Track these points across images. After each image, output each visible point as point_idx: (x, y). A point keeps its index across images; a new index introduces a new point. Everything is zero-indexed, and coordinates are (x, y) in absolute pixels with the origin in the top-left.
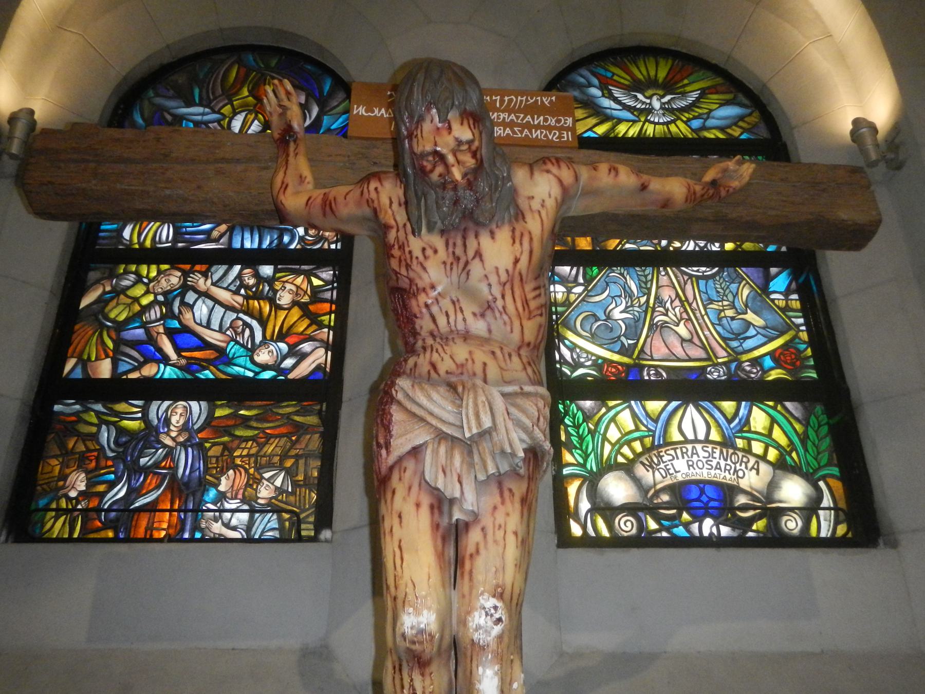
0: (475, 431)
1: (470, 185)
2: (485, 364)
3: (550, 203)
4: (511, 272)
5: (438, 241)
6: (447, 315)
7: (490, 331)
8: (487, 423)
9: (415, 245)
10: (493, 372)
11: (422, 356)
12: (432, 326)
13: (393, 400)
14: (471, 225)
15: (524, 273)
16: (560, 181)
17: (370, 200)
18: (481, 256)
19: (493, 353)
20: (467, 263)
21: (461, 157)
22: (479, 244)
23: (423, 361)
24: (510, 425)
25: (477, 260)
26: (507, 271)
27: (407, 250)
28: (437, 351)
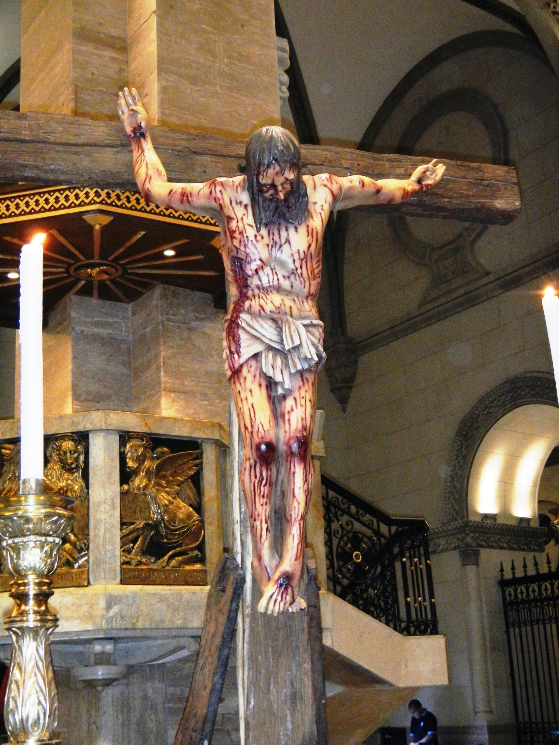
0: (291, 346)
1: (286, 199)
2: (291, 307)
3: (327, 207)
4: (306, 253)
5: (264, 231)
6: (268, 275)
7: (292, 287)
8: (297, 342)
9: (251, 232)
10: (295, 312)
11: (253, 300)
12: (258, 283)
13: (238, 326)
14: (282, 222)
15: (313, 253)
16: (332, 192)
17: (217, 198)
18: (289, 243)
19: (294, 300)
20: (281, 246)
21: (285, 186)
22: (288, 235)
23: (255, 304)
24: (309, 343)
25: (287, 244)
26: (304, 252)
27: (245, 235)
28: (262, 298)
